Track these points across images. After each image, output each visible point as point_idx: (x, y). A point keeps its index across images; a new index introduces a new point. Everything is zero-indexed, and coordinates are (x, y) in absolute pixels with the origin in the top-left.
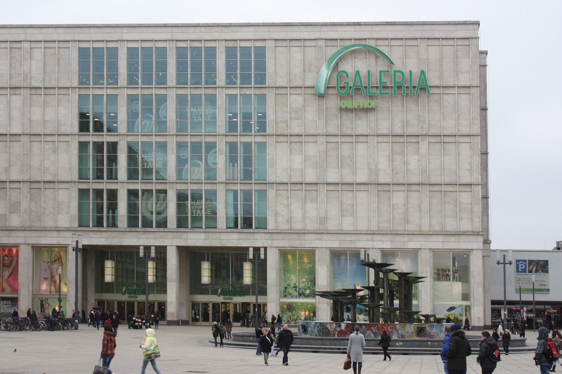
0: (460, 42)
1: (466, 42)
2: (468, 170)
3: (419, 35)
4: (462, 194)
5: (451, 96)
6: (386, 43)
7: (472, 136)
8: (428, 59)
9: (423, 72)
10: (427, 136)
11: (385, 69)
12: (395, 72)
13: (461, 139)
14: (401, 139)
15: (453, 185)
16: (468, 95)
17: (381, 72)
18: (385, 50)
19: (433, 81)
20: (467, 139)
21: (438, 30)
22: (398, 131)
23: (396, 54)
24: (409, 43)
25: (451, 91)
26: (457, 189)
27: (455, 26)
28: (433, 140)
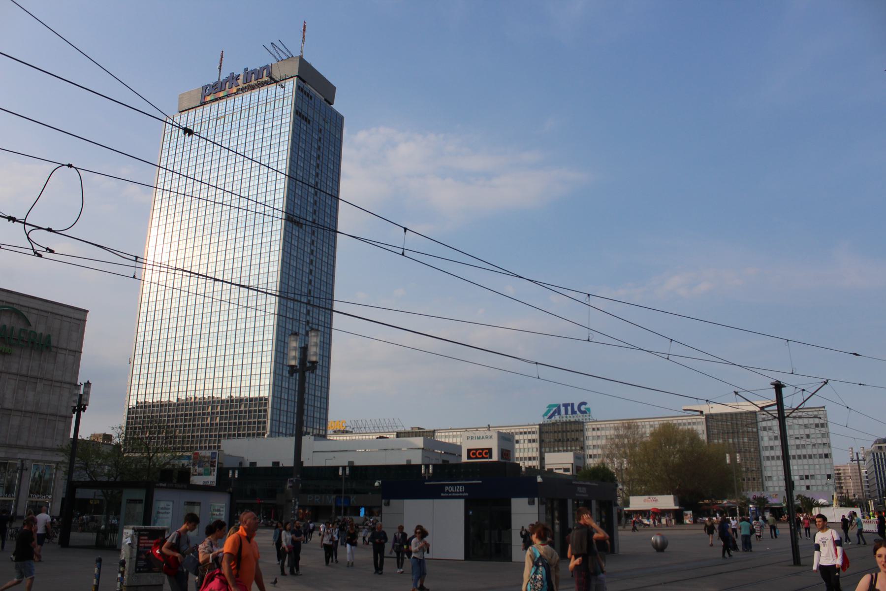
1: (78, 322)
3: (50, 310)
6: (27, 310)
9: (49, 336)
11: (22, 327)
12: (31, 331)
13: (65, 386)
14: (25, 379)
16: (73, 357)
17: (21, 329)
18: (25, 314)
19: (54, 342)
20: (68, 386)
22: (24, 372)
23: (32, 319)
24: (43, 314)
25: (64, 352)
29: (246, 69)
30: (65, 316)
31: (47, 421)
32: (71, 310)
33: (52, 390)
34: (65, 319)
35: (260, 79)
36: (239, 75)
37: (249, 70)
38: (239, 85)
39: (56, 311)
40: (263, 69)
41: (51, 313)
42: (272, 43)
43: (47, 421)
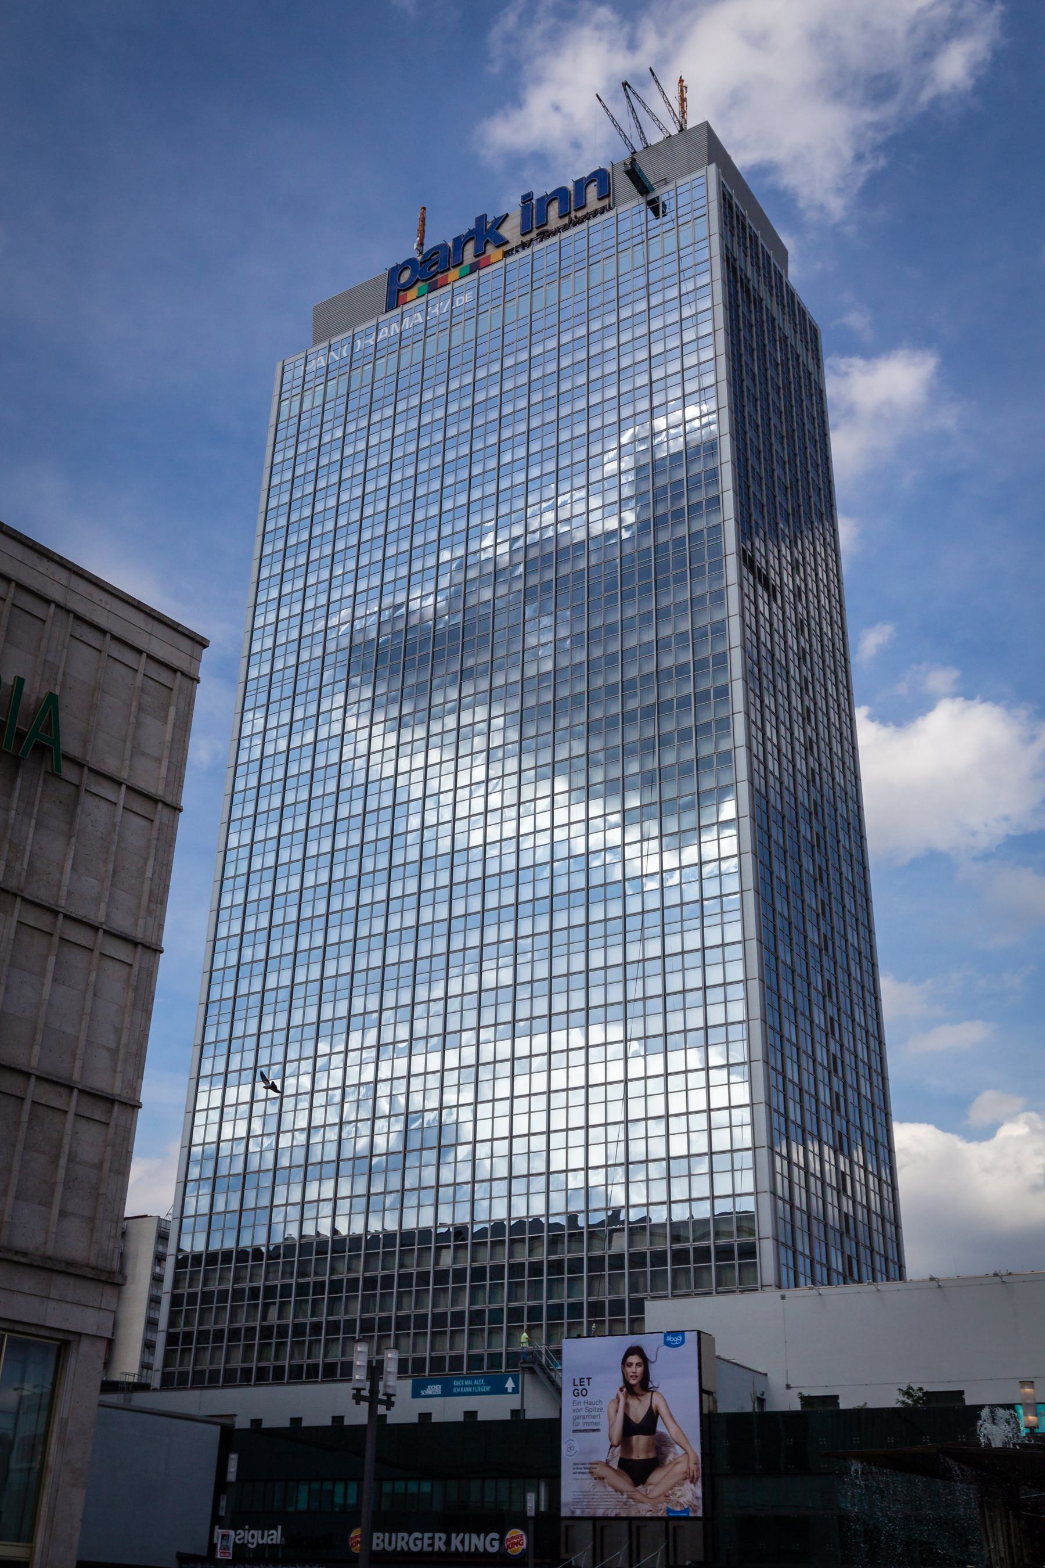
0: (155, 671)
2: (108, 1049)
3: (56, 593)
4: (83, 1124)
5: (104, 806)
7: (140, 948)
8: (64, 674)
9: (52, 699)
10: (19, 900)
15: (59, 1089)
16: (144, 823)
21: (108, 607)
25: (106, 790)
26: (68, 1104)
27: (150, 620)
28: (33, 917)
29: (527, 198)
30: (114, 638)
31: (27, 1105)
32: (139, 619)
33: (52, 960)
34: (116, 650)
35: (576, 210)
36: (507, 215)
37: (536, 197)
38: (507, 242)
39: (81, 608)
40: (581, 185)
41: (58, 606)
42: (625, 84)
43: (27, 1105)
